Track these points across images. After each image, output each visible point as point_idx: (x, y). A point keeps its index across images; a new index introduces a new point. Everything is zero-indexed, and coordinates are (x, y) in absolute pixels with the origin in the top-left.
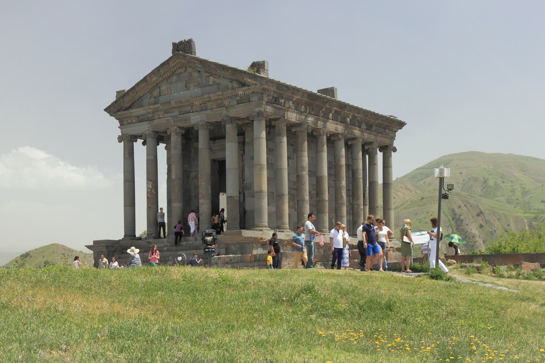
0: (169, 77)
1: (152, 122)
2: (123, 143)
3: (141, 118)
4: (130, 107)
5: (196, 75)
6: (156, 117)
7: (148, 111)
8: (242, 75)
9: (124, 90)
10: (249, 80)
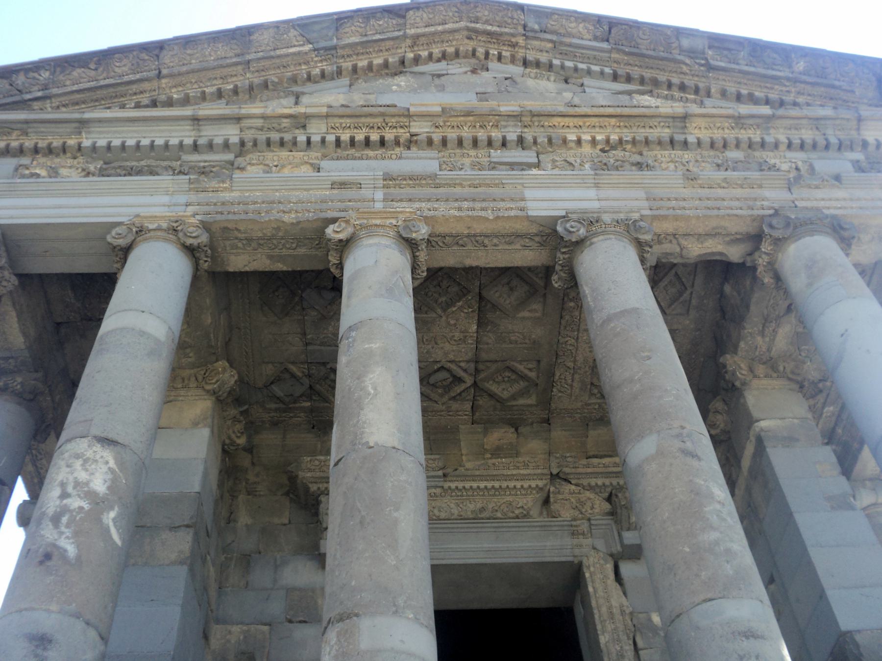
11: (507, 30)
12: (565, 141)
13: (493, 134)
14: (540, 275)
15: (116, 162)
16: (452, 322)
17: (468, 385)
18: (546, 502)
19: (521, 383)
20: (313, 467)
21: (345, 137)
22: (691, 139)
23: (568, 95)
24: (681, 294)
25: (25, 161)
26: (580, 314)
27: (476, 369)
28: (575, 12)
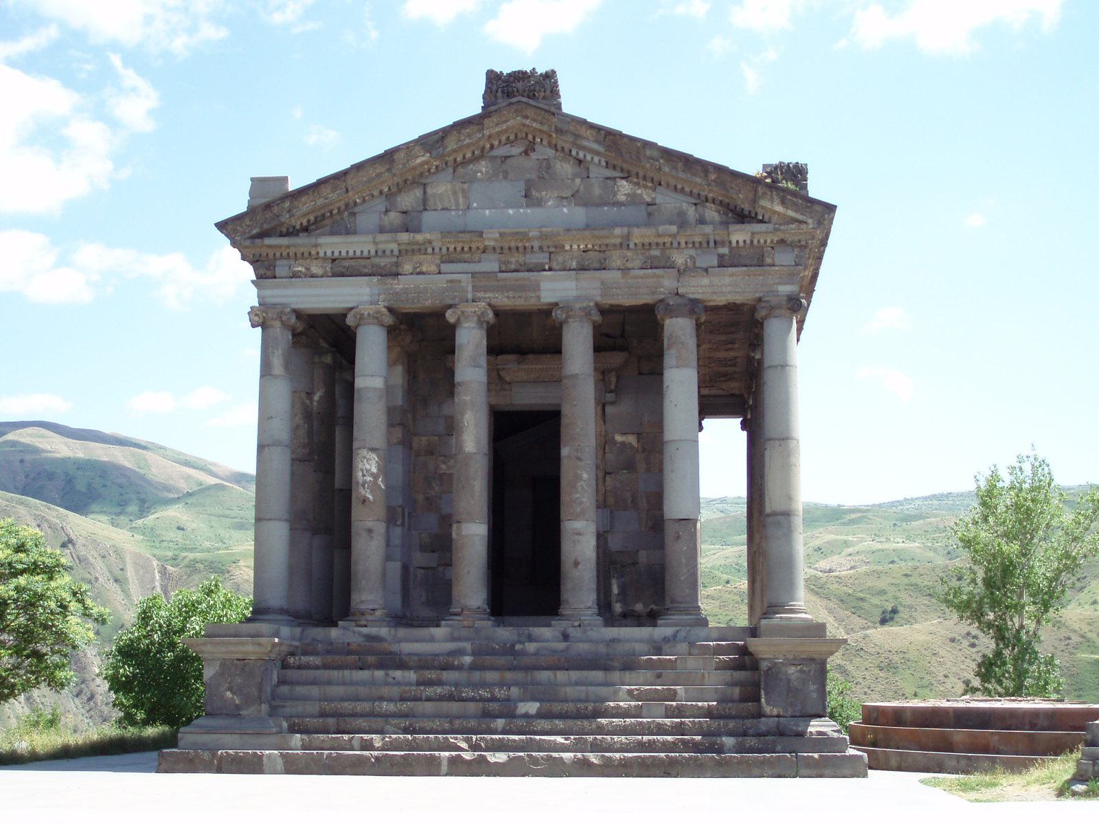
0: (465, 162)
1: (389, 280)
2: (259, 329)
3: (346, 264)
4: (305, 229)
5: (565, 168)
6: (408, 267)
7: (382, 247)
8: (756, 191)
9: (285, 179)
10: (779, 208)
11: (545, 128)
12: (564, 247)
13: (527, 245)
15: (342, 269)
21: (452, 247)
22: (632, 246)
23: (578, 181)
25: (292, 262)
28: (584, 122)
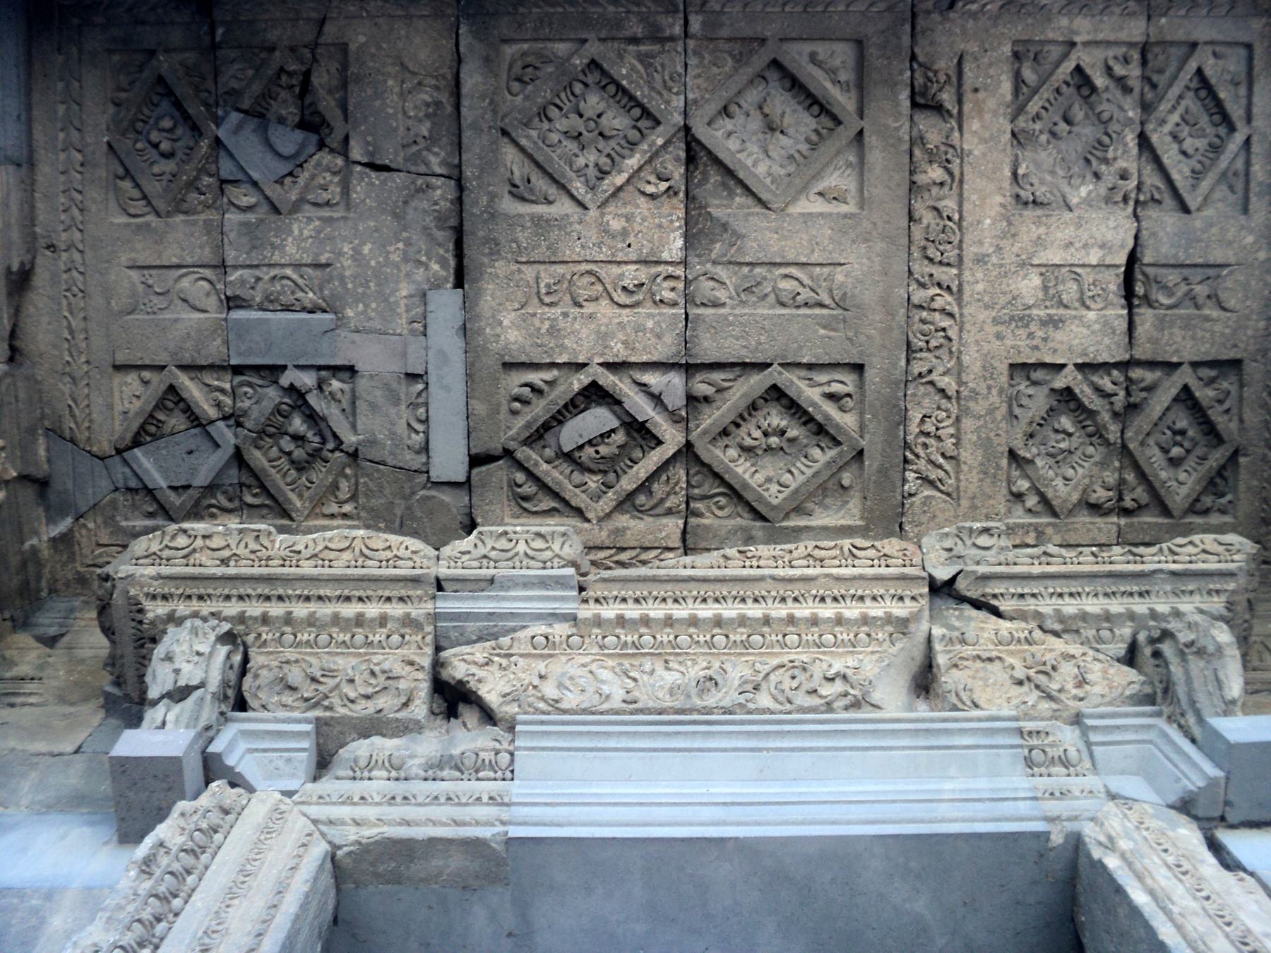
14: (843, 77)
16: (616, 225)
17: (668, 450)
18: (924, 681)
19: (816, 453)
20: (166, 553)
24: (1216, 148)
26: (960, 205)
27: (693, 400)
